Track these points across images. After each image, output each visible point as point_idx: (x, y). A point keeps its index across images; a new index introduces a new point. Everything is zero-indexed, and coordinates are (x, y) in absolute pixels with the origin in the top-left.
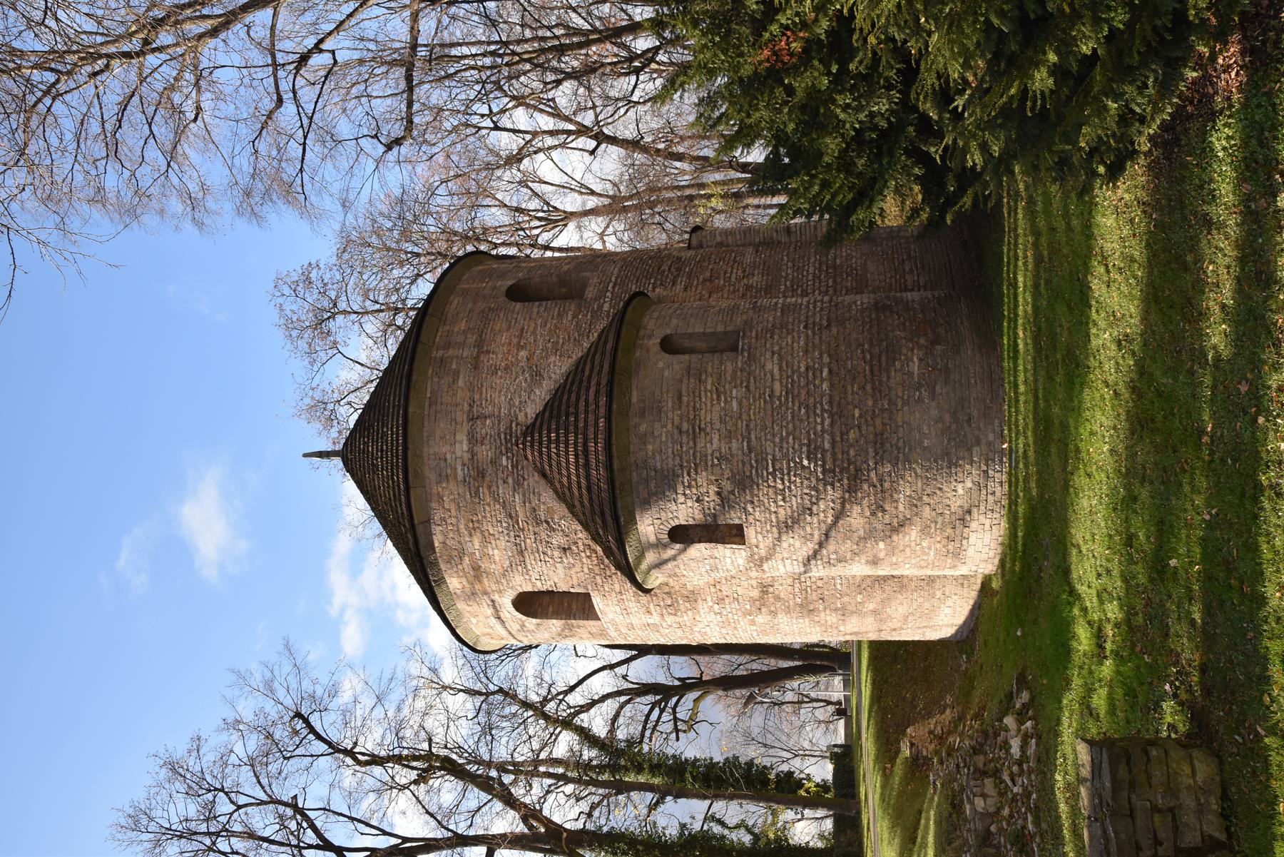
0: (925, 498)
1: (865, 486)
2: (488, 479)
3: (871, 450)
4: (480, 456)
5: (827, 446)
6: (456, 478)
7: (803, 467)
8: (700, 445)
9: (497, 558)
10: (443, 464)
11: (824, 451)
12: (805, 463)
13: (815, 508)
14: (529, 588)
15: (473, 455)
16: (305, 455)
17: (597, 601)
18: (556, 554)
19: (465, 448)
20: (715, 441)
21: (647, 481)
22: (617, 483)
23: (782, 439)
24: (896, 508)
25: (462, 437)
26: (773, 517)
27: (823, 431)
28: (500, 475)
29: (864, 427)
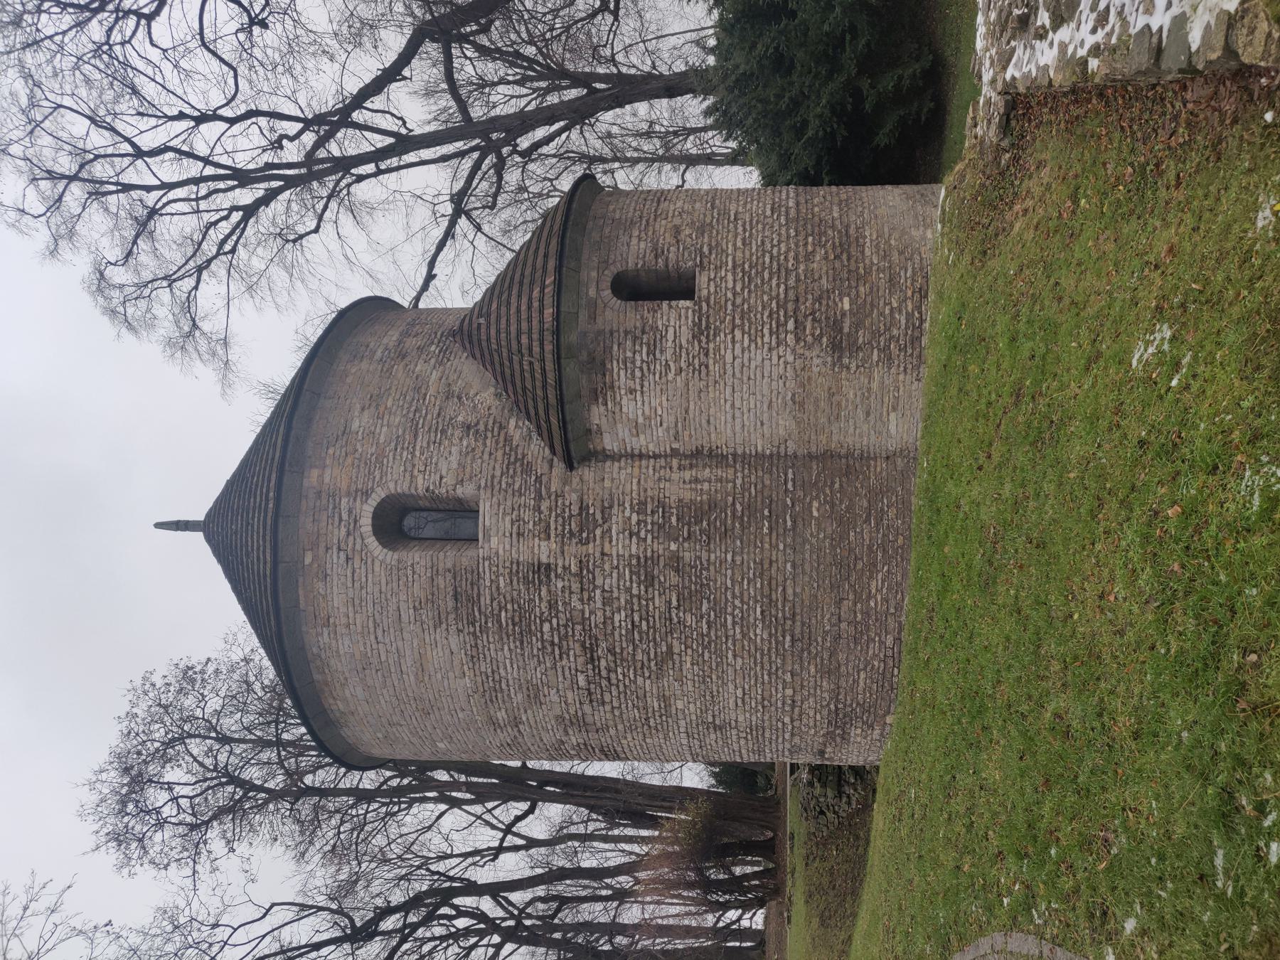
0: (893, 242)
1: (830, 232)
2: (408, 359)
3: (836, 208)
4: (407, 345)
5: (791, 204)
6: (371, 359)
7: (765, 217)
8: (664, 205)
9: (382, 439)
10: (363, 348)
11: (788, 208)
12: (768, 213)
13: (775, 251)
14: (403, 487)
15: (400, 342)
16: (159, 525)
17: (485, 508)
18: (458, 433)
19: (394, 338)
20: (679, 204)
21: (602, 228)
22: (572, 217)
23: (746, 203)
24: (863, 252)
25: (394, 336)
26: (730, 258)
27: (788, 198)
28: (424, 356)
29: (829, 198)
